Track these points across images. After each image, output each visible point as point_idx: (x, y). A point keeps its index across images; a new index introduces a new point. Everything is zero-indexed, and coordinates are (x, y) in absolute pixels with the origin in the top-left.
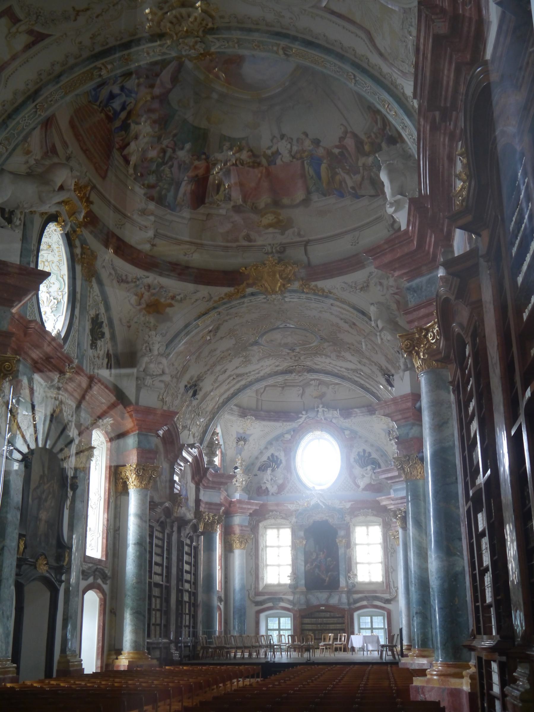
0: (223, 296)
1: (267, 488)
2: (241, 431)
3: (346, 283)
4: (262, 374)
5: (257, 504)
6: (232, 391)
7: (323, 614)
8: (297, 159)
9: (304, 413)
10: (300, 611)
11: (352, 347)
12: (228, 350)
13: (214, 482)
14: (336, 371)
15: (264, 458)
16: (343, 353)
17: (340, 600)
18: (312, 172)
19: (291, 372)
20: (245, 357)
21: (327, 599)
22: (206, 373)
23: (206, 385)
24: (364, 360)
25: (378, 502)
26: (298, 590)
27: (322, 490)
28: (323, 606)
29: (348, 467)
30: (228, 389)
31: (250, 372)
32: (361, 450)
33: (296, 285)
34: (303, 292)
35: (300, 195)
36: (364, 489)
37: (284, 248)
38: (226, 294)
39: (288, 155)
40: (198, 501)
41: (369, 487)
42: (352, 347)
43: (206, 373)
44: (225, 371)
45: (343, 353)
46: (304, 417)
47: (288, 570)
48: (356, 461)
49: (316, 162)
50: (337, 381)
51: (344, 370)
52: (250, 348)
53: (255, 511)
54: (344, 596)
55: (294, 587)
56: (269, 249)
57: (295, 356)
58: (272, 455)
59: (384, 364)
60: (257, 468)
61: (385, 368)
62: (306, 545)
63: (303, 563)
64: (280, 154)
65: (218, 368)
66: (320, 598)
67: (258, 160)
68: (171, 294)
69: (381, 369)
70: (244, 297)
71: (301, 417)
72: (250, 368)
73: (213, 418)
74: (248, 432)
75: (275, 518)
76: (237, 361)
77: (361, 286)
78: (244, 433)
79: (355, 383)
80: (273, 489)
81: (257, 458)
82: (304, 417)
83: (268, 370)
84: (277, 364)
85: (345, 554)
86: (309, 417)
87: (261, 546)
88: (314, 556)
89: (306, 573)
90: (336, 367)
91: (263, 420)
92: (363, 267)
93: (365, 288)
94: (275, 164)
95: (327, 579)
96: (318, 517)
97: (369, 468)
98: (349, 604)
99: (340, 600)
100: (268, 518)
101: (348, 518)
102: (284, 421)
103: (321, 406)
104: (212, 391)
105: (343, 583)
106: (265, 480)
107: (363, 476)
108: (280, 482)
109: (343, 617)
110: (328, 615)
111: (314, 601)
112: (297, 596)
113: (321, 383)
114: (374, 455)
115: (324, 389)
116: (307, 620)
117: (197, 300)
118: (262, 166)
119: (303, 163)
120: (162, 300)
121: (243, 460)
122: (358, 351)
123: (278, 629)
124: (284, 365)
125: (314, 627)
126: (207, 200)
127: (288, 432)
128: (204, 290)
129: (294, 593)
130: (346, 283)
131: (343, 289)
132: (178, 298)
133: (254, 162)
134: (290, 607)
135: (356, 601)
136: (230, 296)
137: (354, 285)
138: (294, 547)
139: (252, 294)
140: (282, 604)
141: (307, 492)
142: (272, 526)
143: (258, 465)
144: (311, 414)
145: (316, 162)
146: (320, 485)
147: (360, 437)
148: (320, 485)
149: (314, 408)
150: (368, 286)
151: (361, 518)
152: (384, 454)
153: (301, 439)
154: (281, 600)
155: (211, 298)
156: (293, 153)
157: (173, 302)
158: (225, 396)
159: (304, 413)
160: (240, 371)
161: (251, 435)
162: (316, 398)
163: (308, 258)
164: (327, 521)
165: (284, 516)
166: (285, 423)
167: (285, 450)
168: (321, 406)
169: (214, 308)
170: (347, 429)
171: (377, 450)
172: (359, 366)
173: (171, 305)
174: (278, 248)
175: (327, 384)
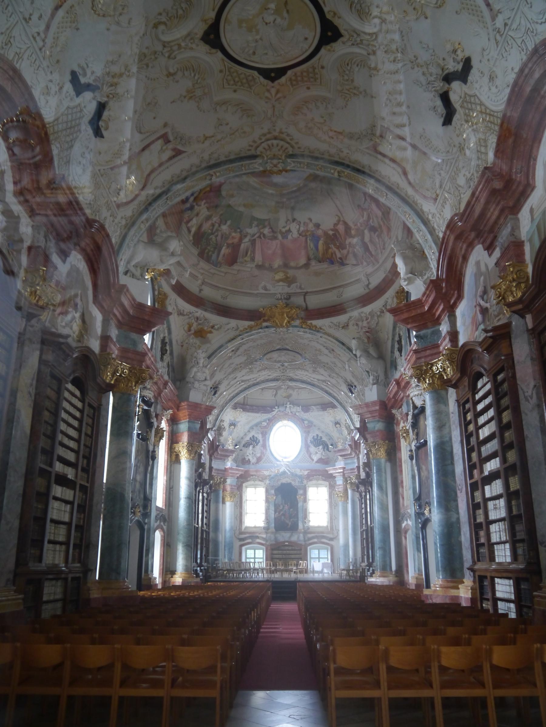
0: (246, 327)
1: (249, 459)
2: (232, 419)
3: (332, 323)
4: (258, 381)
5: (242, 471)
6: (236, 392)
7: (287, 548)
8: (303, 236)
9: (276, 407)
10: (271, 545)
11: (327, 365)
12: (240, 364)
13: (221, 455)
14: (309, 380)
15: (247, 438)
16: (318, 369)
17: (298, 538)
18: (312, 245)
20: (250, 369)
21: (290, 537)
22: (224, 379)
23: (222, 388)
24: (334, 375)
25: (327, 471)
26: (270, 531)
27: (288, 462)
28: (287, 542)
29: (306, 446)
30: (234, 391)
31: (250, 379)
32: (315, 435)
33: (297, 322)
34: (302, 327)
35: (303, 261)
36: (317, 462)
37: (290, 296)
38: (249, 326)
39: (296, 233)
40: (211, 468)
41: (320, 461)
42: (327, 365)
43: (224, 379)
44: (235, 378)
45: (318, 369)
46: (277, 410)
47: (263, 517)
48: (311, 442)
49: (316, 239)
50: (309, 387)
52: (254, 363)
53: (241, 475)
54: (301, 535)
55: (266, 529)
58: (253, 436)
59: (350, 378)
60: (242, 445)
61: (349, 381)
62: (275, 500)
63: (273, 512)
65: (232, 376)
66: (284, 536)
67: (276, 235)
68: (211, 324)
69: (346, 381)
70: (261, 328)
71: (274, 411)
72: (251, 376)
73: (222, 410)
74: (237, 420)
75: (254, 481)
76: (244, 371)
78: (235, 420)
79: (322, 389)
80: (253, 460)
81: (242, 438)
82: (277, 410)
83: (262, 378)
84: (269, 374)
85: (303, 506)
86: (280, 411)
87: (244, 500)
88: (281, 507)
89: (275, 519)
91: (248, 411)
92: (345, 312)
93: (346, 326)
95: (290, 524)
96: (284, 481)
97: (321, 447)
98: (305, 541)
99: (298, 538)
100: (249, 481)
101: (305, 482)
102: (262, 413)
103: (288, 403)
104: (225, 391)
105: (301, 526)
106: (248, 454)
107: (317, 453)
108: (258, 455)
109: (301, 550)
110: (290, 548)
111: (281, 539)
112: (269, 535)
113: (289, 387)
114: (324, 439)
115: (291, 392)
116: (275, 552)
117: (228, 329)
118: (278, 239)
119: (306, 239)
120: (206, 328)
121: (233, 440)
123: (255, 557)
124: (274, 375)
125: (280, 556)
126: (238, 261)
127: (265, 421)
128: (233, 323)
129: (266, 533)
130: (332, 323)
132: (216, 327)
134: (263, 542)
135: (310, 539)
136: (251, 328)
138: (267, 501)
139: (267, 327)
140: (258, 540)
141: (278, 463)
142: (251, 486)
143: (243, 443)
144: (281, 409)
146: (285, 458)
147: (315, 426)
148: (285, 458)
149: (283, 405)
150: (347, 326)
151: (314, 482)
152: (331, 438)
153: (273, 426)
154: (258, 537)
155: (238, 328)
157: (212, 330)
158: (232, 395)
159: (276, 407)
160: (245, 378)
161: (239, 422)
162: (285, 397)
163: (306, 304)
164: (290, 484)
165: (261, 479)
166: (263, 415)
167: (262, 433)
168: (288, 403)
169: (240, 335)
170: (306, 420)
171: (326, 435)
172: (328, 378)
173: (211, 332)
175: (293, 388)
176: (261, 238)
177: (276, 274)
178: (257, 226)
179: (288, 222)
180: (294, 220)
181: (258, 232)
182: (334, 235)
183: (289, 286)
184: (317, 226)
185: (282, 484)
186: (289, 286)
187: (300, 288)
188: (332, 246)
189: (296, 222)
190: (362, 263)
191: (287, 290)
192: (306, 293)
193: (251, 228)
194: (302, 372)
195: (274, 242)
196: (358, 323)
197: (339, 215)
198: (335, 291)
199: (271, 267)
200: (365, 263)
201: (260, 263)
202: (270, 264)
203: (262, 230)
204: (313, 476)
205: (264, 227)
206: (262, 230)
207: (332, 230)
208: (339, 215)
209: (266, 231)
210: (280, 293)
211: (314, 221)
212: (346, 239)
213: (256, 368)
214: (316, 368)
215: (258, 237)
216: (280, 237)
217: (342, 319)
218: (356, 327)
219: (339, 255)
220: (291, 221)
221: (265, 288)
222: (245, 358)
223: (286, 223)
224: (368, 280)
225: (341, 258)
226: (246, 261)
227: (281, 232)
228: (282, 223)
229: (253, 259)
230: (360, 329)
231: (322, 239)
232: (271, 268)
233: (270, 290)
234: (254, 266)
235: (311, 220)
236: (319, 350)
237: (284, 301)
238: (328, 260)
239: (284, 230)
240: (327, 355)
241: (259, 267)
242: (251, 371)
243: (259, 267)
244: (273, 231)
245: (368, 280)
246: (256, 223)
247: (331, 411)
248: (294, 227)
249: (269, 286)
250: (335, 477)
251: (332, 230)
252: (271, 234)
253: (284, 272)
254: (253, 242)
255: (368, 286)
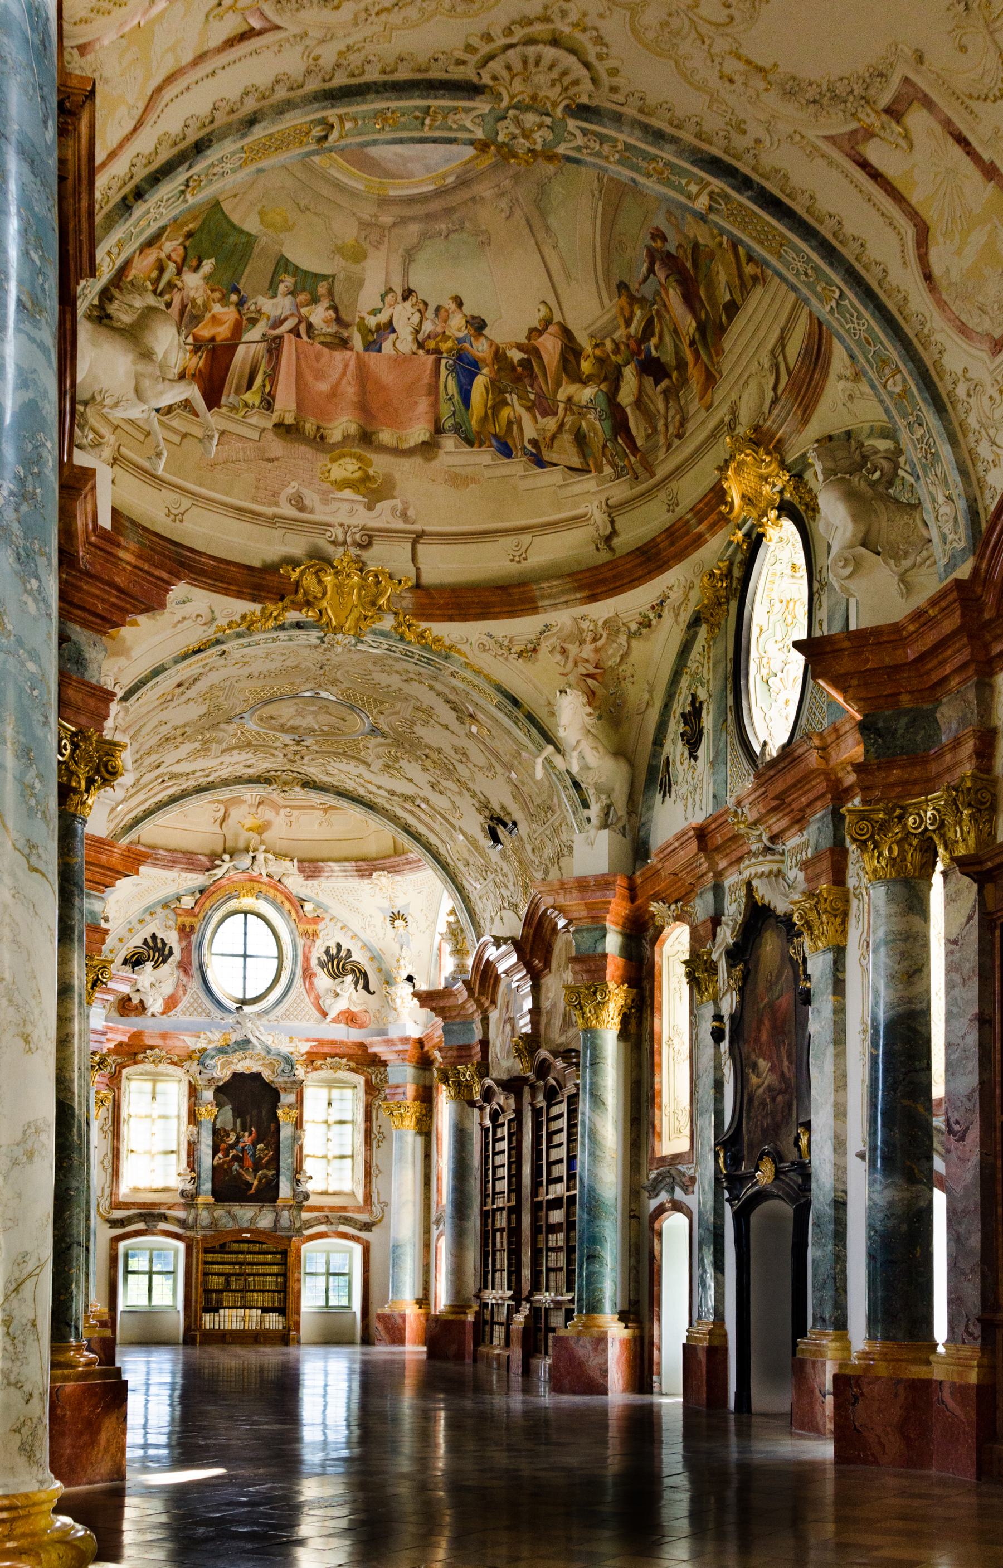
3: (490, 636)
12: (184, 726)
19: (268, 781)
20: (205, 742)
30: (146, 800)
39: (410, 338)
51: (386, 794)
52: (222, 726)
56: (338, 533)
57: (295, 753)
64: (394, 331)
67: (346, 334)
76: (188, 747)
77: (522, 648)
90: (369, 786)
94: (380, 350)
118: (352, 350)
122: (449, 771)
130: (490, 636)
131: (483, 647)
133: (335, 335)
137: (506, 643)
145: (466, 369)
150: (535, 650)
151: (324, 1073)
156: (420, 337)
163: (418, 569)
164: (259, 1075)
174: (357, 537)
176: (299, 336)
177: (333, 460)
178: (292, 293)
179: (389, 298)
180: (408, 294)
181: (292, 315)
182: (526, 364)
183: (370, 508)
184: (478, 325)
185: (235, 1075)
186: (370, 508)
187: (404, 516)
188: (515, 397)
189: (412, 299)
190: (600, 469)
191: (363, 518)
192: (420, 536)
193: (274, 296)
194: (353, 768)
195: (339, 356)
196: (565, 645)
197: (552, 302)
198: (507, 543)
199: (322, 437)
200: (608, 470)
201: (289, 420)
202: (318, 428)
203: (304, 311)
204: (325, 1056)
205: (315, 300)
206: (304, 311)
207: (520, 347)
208: (552, 302)
209: (319, 315)
210: (342, 525)
211: (469, 309)
212: (558, 384)
213: (219, 742)
214: (396, 759)
215: (290, 331)
216: (357, 342)
217: (521, 628)
218: (558, 657)
219: (530, 432)
220: (399, 293)
221: (299, 502)
222: (203, 709)
223: (383, 300)
224: (612, 522)
225: (534, 442)
226: (246, 405)
227: (365, 331)
228: (368, 298)
229: (268, 403)
230: (570, 664)
231: (485, 371)
232: (319, 441)
233: (312, 512)
234: (270, 426)
235: (459, 303)
236: (429, 712)
237: (353, 551)
238: (494, 443)
239: (372, 322)
240: (446, 727)
241: (283, 429)
242: (205, 749)
243: (286, 430)
244: (339, 320)
245: (612, 522)
246: (288, 282)
247: (381, 878)
248: (404, 316)
249: (311, 498)
250: (385, 1064)
251: (520, 347)
252: (333, 329)
253: (359, 458)
254: (274, 346)
255: (608, 539)
